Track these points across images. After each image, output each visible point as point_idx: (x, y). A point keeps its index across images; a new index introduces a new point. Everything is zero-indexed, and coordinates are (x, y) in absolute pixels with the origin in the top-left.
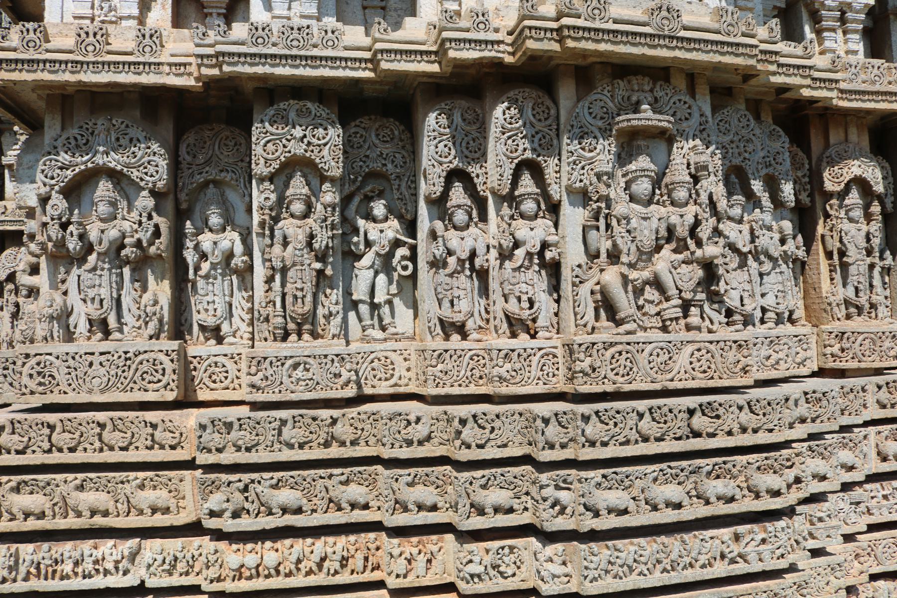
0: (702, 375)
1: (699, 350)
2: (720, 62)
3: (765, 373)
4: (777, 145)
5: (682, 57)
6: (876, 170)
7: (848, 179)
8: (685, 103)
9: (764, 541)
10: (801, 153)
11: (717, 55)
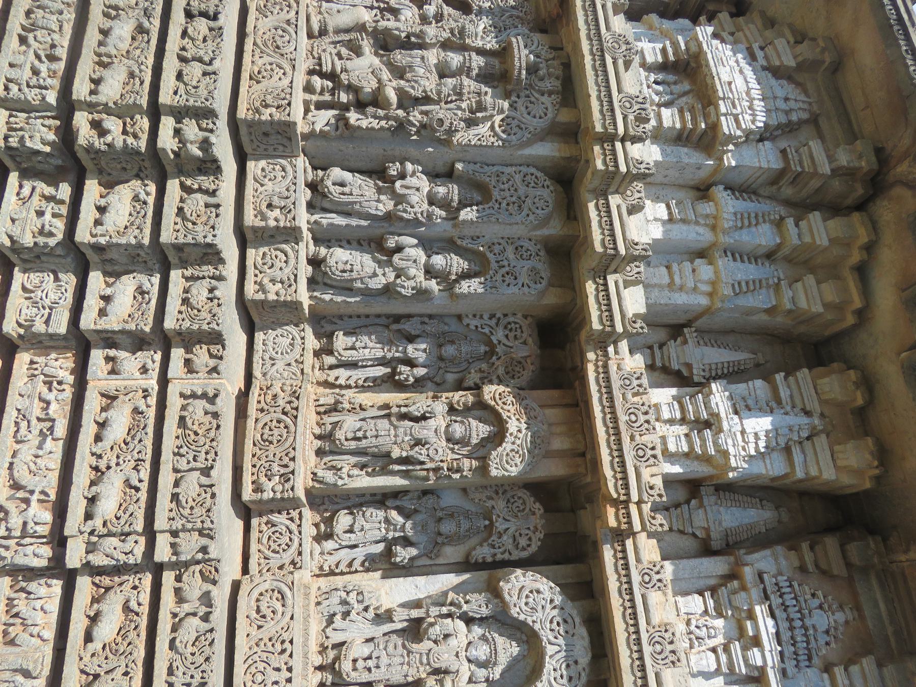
0: (256, 70)
1: (284, 74)
2: (590, 96)
3: (252, 200)
4: (524, 278)
5: (585, 61)
6: (518, 460)
7: (501, 411)
8: (546, 115)
9: (36, 72)
10: (526, 375)
11: (596, 93)
